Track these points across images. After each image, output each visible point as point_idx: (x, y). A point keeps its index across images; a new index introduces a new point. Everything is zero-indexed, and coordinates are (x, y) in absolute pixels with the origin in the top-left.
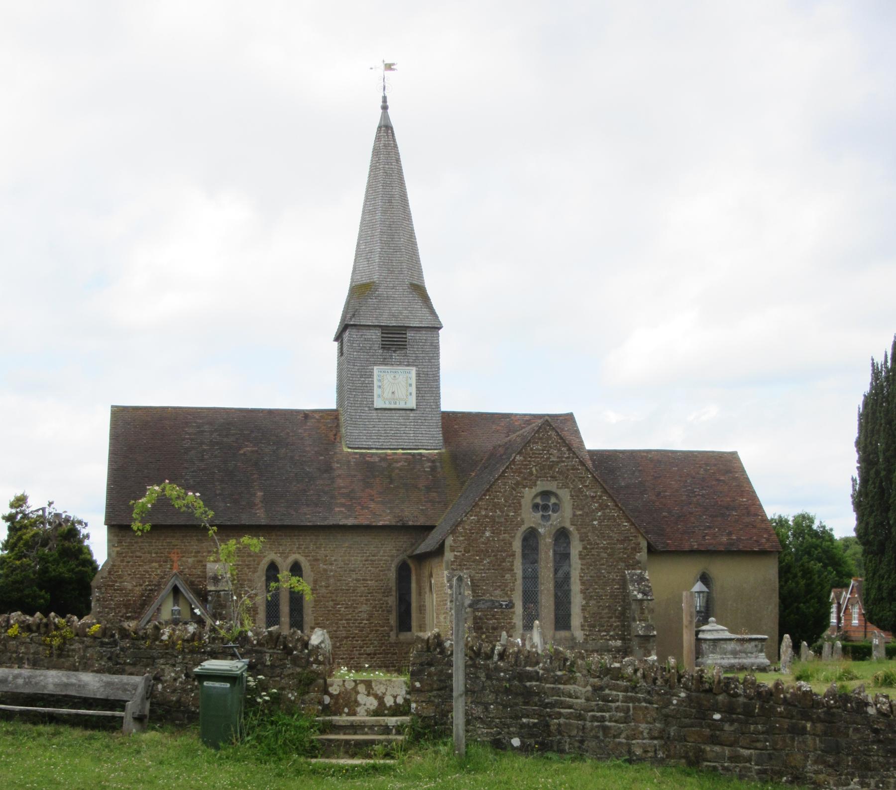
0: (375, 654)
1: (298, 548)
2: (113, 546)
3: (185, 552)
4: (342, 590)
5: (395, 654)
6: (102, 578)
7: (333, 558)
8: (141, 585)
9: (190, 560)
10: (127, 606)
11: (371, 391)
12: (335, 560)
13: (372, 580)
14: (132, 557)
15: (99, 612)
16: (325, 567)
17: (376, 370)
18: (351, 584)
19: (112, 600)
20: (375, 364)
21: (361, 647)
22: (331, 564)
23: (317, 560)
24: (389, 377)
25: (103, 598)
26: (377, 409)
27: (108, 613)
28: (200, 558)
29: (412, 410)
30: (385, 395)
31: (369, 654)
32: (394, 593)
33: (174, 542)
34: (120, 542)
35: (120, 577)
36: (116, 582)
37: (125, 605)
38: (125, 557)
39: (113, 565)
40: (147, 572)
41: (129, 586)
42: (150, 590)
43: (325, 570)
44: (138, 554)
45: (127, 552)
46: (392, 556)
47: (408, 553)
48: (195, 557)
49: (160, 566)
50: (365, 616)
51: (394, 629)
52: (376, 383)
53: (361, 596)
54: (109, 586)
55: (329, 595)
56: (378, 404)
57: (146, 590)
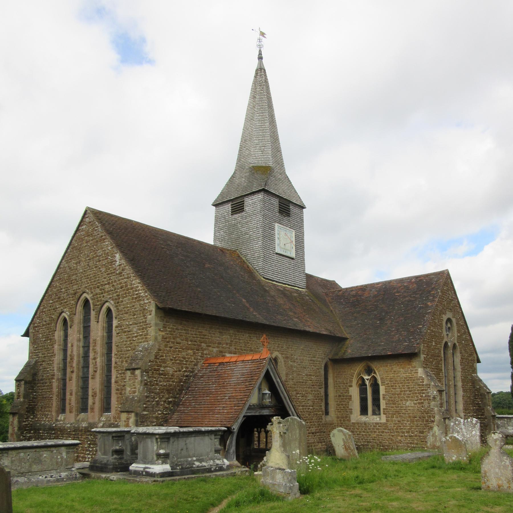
0: (316, 433)
1: (278, 347)
2: (160, 330)
3: (210, 343)
4: (300, 382)
5: (324, 432)
6: (150, 361)
7: (296, 357)
8: (180, 371)
9: (215, 350)
10: (168, 391)
11: (274, 240)
12: (297, 359)
13: (313, 376)
14: (173, 343)
15: (147, 397)
16: (291, 363)
17: (277, 225)
18: (304, 378)
19: (157, 384)
20: (275, 222)
21: (310, 428)
22: (294, 362)
23: (287, 358)
24: (282, 233)
25: (151, 382)
26: (277, 254)
27: (154, 398)
28: (221, 349)
29: (293, 259)
30: (281, 245)
31: (313, 433)
32: (323, 386)
33: (205, 332)
34: (164, 327)
35: (164, 361)
36: (161, 366)
37: (167, 390)
38: (168, 342)
39: (160, 350)
40: (184, 358)
41: (170, 370)
42: (187, 376)
43: (292, 366)
44: (178, 340)
45: (170, 338)
46: (322, 358)
47: (330, 357)
48: (218, 347)
49: (194, 354)
50: (310, 403)
51: (324, 413)
52: (277, 236)
53: (309, 388)
54: (155, 370)
55: (294, 386)
56: (278, 250)
57: (183, 376)
